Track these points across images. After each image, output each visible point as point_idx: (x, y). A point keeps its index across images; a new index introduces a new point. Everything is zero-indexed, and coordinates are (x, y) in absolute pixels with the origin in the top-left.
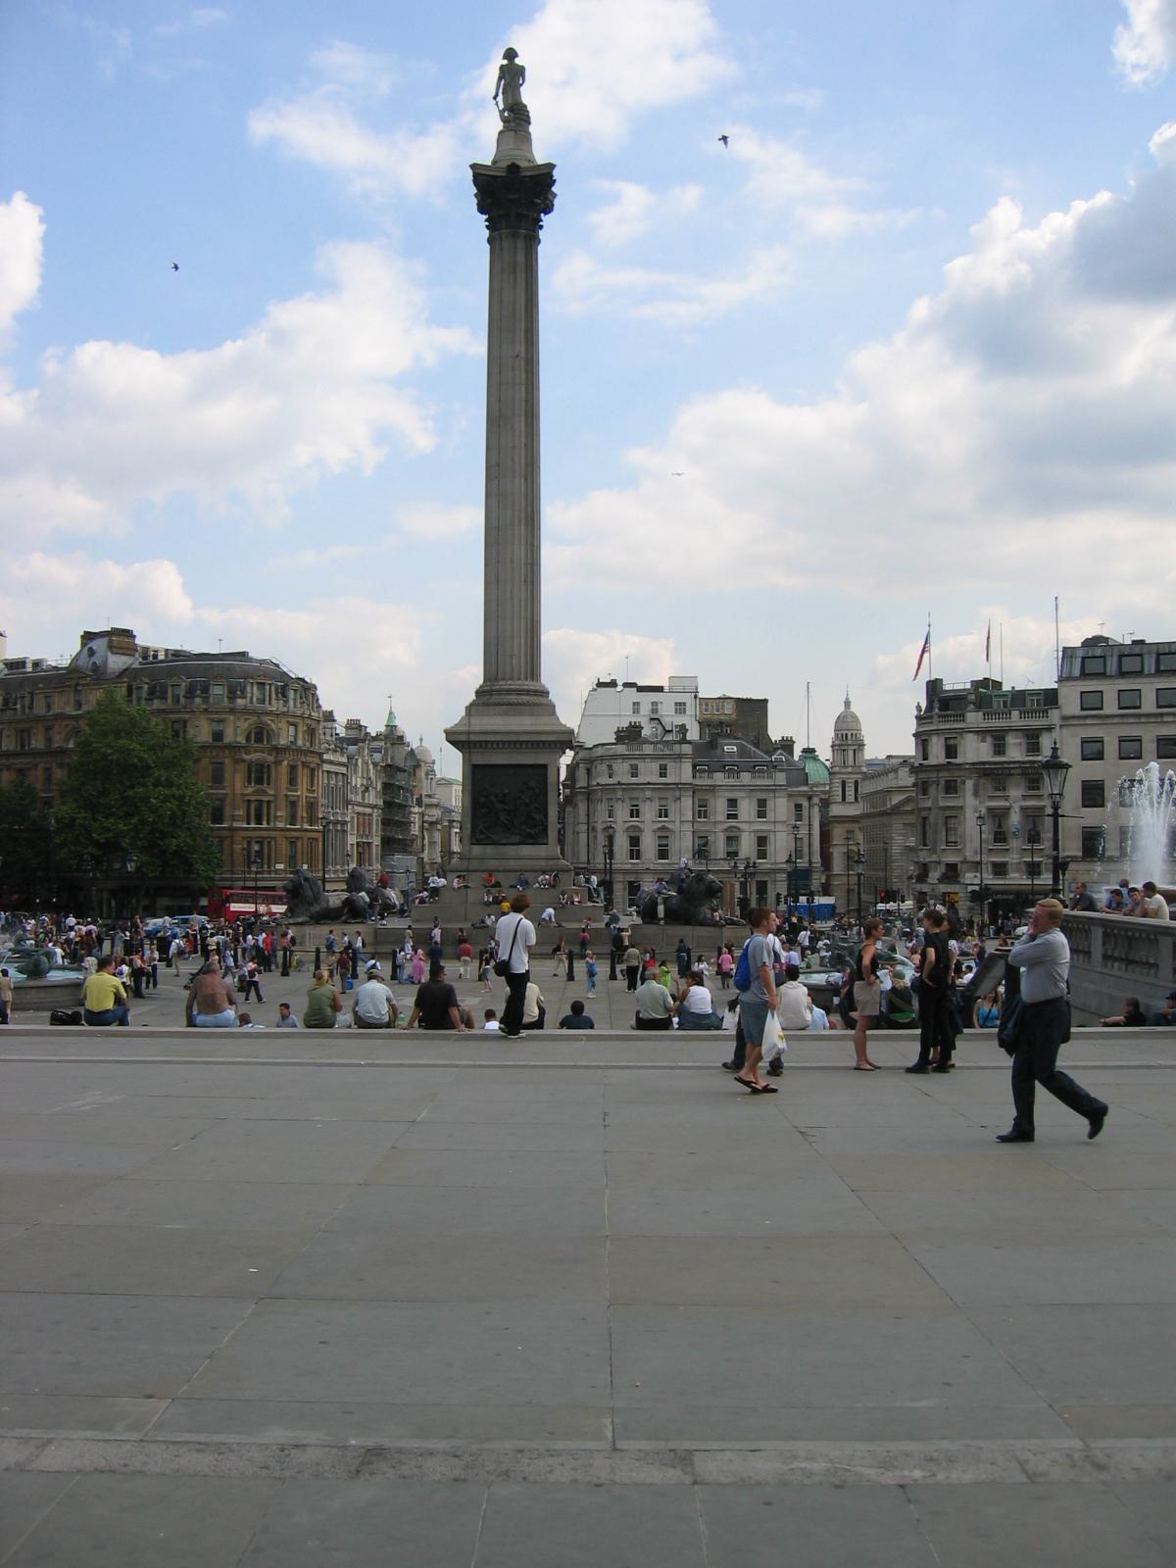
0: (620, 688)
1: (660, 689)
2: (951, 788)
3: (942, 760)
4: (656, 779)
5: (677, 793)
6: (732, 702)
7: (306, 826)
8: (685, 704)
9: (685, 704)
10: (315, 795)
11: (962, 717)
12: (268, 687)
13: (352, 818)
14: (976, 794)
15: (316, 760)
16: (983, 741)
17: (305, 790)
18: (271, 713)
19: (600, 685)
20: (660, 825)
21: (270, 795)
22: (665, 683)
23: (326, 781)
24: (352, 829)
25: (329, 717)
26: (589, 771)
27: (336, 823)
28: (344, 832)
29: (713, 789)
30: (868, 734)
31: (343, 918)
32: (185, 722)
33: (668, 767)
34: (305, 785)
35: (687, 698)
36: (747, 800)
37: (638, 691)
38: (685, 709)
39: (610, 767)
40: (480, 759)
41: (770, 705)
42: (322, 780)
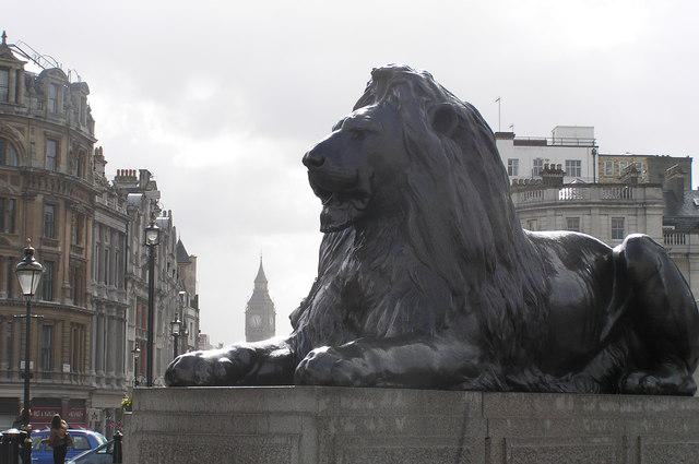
1: (542, 143)
7: (69, 303)
8: (579, 162)
9: (579, 162)
10: (83, 256)
12: (14, 75)
13: (131, 300)
15: (85, 202)
17: (68, 247)
18: (19, 116)
21: (13, 248)
23: (97, 239)
24: (131, 316)
25: (99, 158)
27: (110, 304)
28: (123, 320)
31: (602, 364)
33: (626, 222)
34: (68, 239)
35: (583, 155)
37: (518, 143)
38: (579, 170)
41: (694, 165)
42: (91, 233)
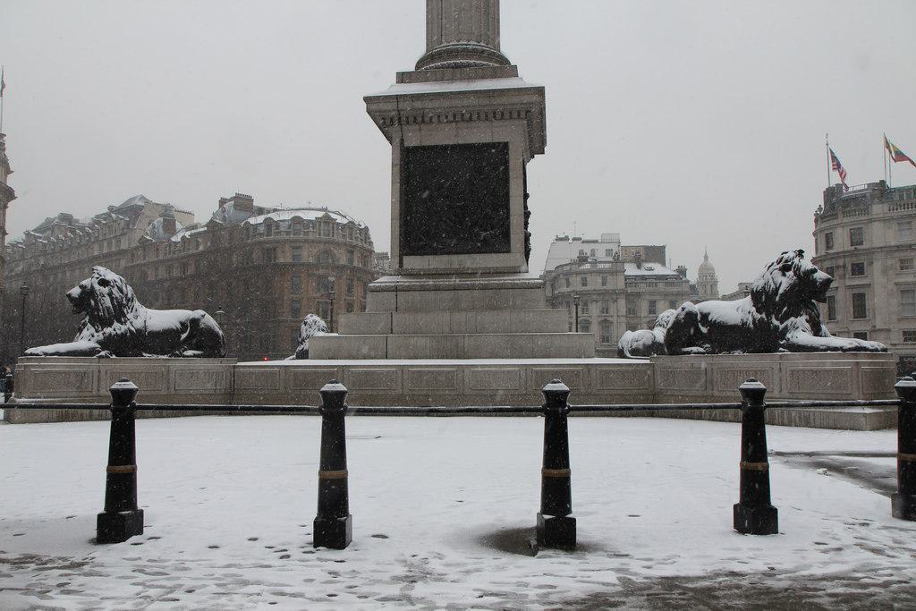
0: (570, 241)
1: (596, 242)
2: (858, 270)
3: (848, 247)
4: (599, 287)
5: (615, 296)
6: (642, 249)
11: (866, 211)
14: (885, 271)
16: (889, 228)
19: (559, 239)
20: (603, 318)
22: (599, 239)
26: (552, 285)
29: (639, 295)
30: (719, 275)
32: (275, 249)
36: (663, 302)
37: (583, 242)
39: (567, 280)
40: (413, 140)
